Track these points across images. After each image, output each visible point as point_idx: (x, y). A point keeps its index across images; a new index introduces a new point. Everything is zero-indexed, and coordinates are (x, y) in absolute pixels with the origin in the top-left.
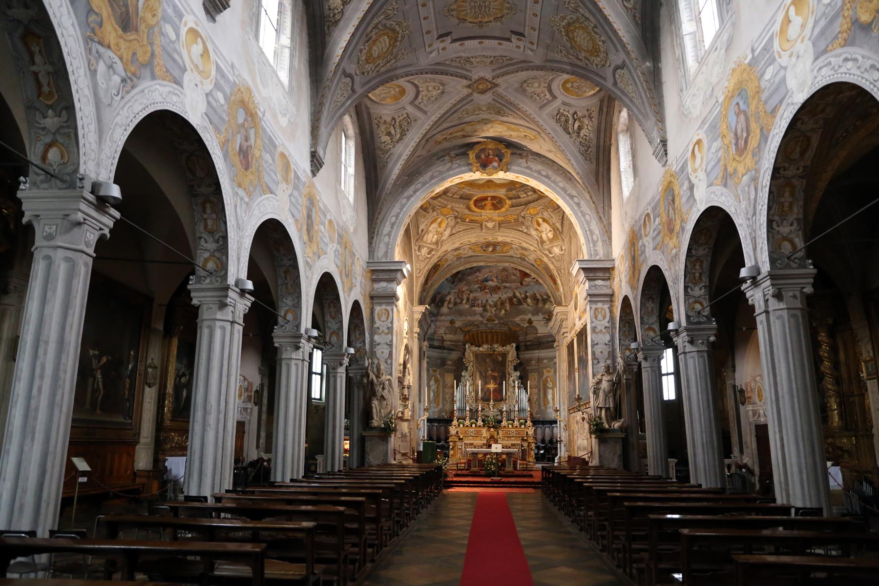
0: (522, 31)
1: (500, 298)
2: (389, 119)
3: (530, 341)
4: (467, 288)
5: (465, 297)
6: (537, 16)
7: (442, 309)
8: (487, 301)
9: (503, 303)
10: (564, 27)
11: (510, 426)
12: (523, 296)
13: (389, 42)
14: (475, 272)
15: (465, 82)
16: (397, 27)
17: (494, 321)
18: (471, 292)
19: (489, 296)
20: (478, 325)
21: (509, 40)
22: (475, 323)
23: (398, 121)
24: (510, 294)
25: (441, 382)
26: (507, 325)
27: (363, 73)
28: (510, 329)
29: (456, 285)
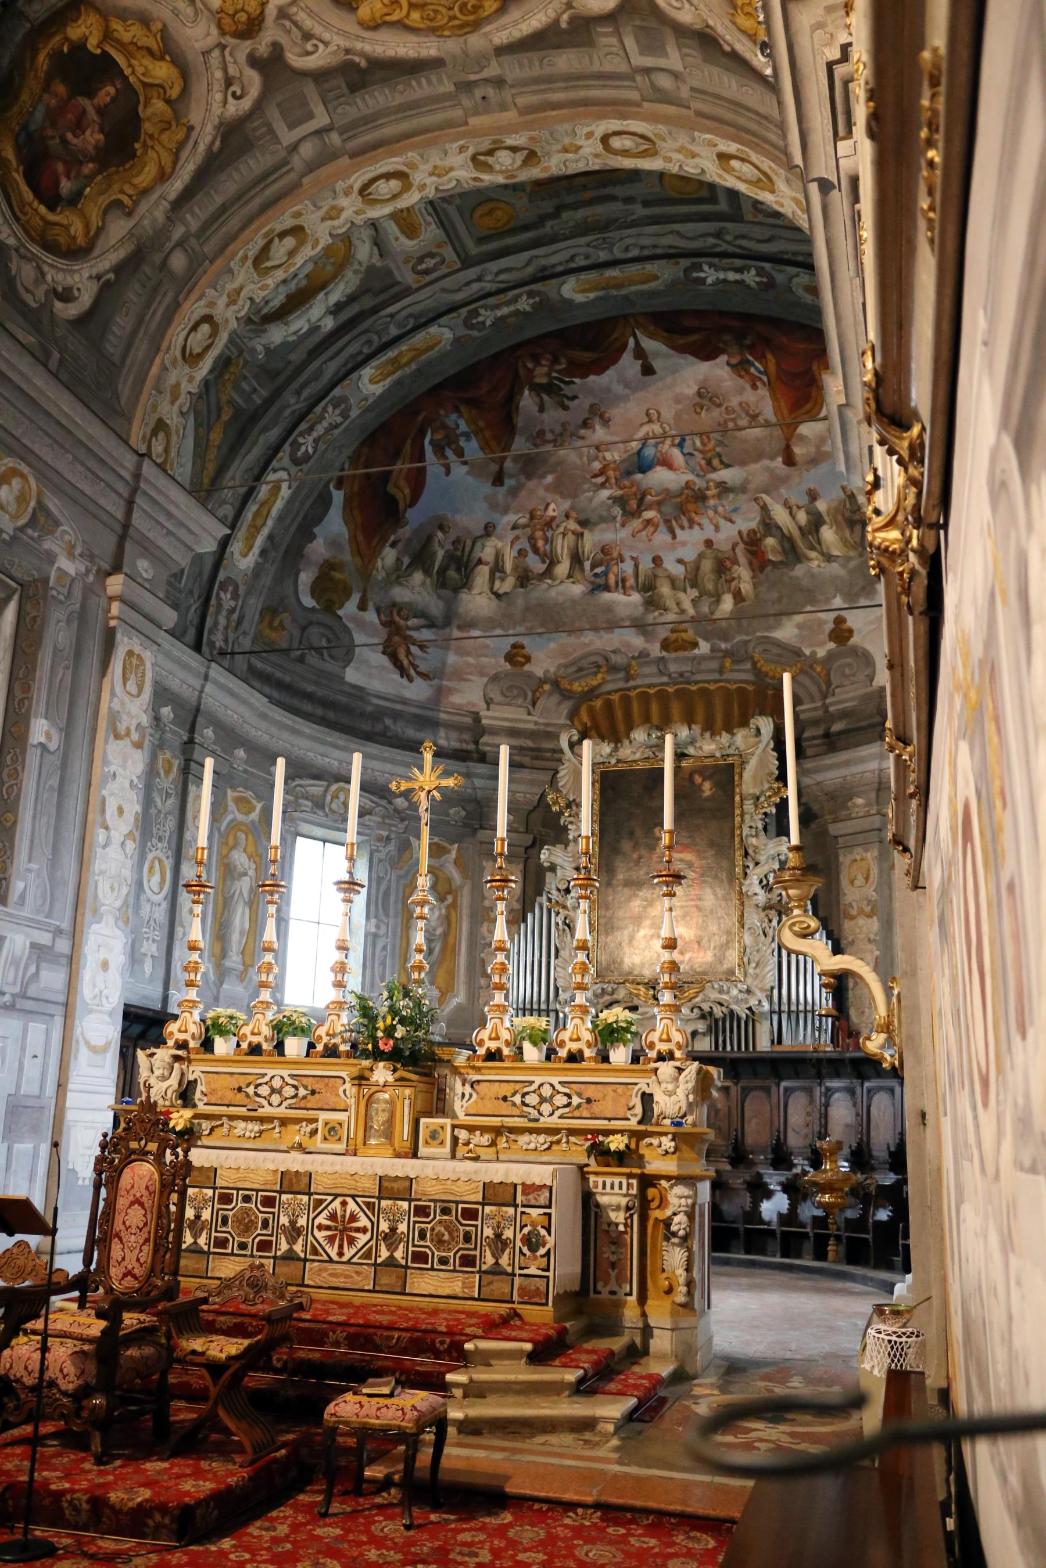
1: (709, 543)
3: (843, 715)
4: (566, 505)
5: (562, 547)
7: (464, 596)
8: (657, 561)
9: (722, 567)
11: (532, 1054)
12: (802, 517)
14: (586, 424)
17: (695, 645)
18: (584, 523)
19: (662, 537)
20: (627, 669)
22: (617, 659)
24: (748, 521)
25: (465, 900)
26: (752, 658)
28: (756, 670)
29: (514, 492)
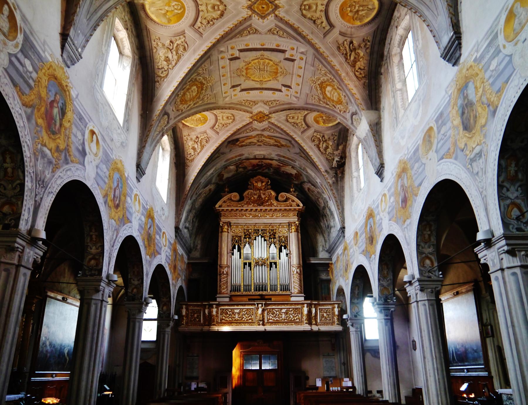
0: (290, 85)
2: (194, 138)
6: (299, 85)
10: (319, 84)
13: (198, 90)
15: (249, 115)
16: (203, 81)
21: (280, 91)
23: (200, 139)
27: (177, 110)
